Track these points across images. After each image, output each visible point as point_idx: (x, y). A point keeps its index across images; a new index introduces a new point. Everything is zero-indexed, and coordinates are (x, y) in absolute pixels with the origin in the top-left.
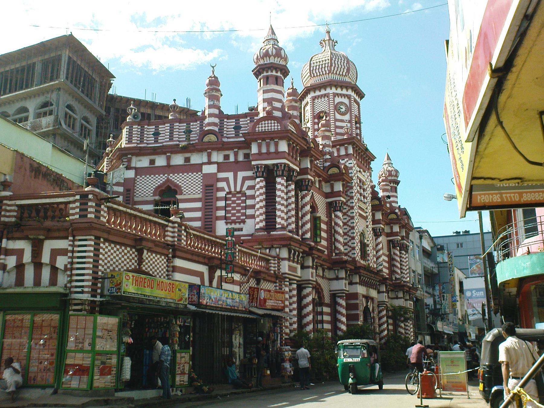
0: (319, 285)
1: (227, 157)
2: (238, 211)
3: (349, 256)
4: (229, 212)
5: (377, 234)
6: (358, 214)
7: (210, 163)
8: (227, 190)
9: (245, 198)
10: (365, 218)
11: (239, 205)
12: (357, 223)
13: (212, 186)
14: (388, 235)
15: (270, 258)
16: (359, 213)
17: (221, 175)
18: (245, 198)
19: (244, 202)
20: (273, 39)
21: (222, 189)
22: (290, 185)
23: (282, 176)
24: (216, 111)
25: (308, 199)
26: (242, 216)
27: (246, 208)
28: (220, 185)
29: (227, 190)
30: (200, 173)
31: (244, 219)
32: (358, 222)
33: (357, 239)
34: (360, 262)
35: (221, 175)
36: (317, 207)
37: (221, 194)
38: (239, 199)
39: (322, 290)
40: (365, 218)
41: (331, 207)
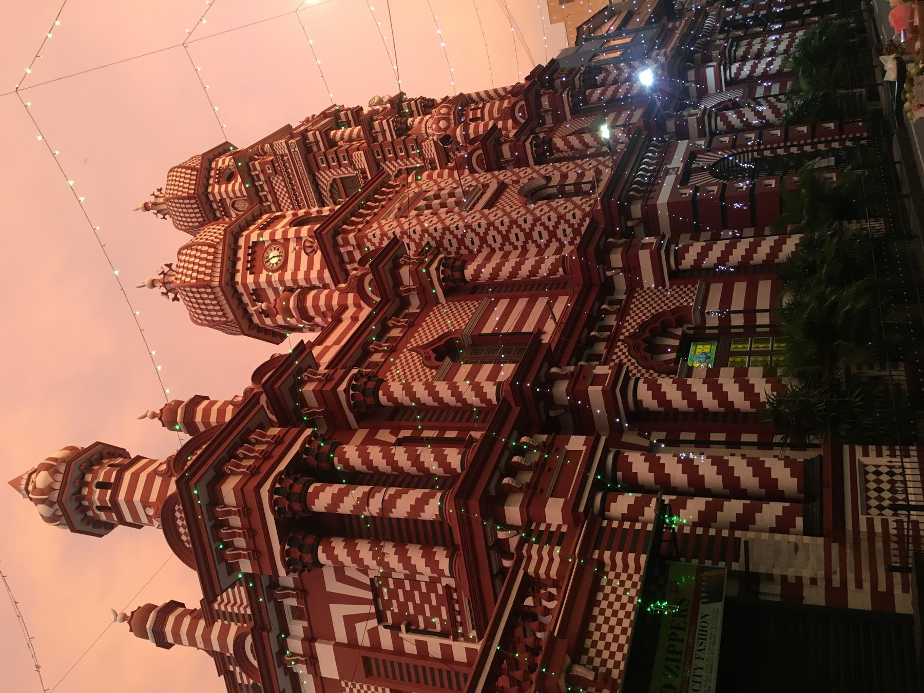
0: (643, 326)
6: (486, 211)
10: (502, 187)
15: (521, 573)
16: (484, 208)
20: (23, 485)
22: (345, 461)
23: (304, 499)
32: (503, 210)
33: (540, 209)
36: (440, 338)
39: (655, 318)
40: (502, 187)
41: (457, 288)
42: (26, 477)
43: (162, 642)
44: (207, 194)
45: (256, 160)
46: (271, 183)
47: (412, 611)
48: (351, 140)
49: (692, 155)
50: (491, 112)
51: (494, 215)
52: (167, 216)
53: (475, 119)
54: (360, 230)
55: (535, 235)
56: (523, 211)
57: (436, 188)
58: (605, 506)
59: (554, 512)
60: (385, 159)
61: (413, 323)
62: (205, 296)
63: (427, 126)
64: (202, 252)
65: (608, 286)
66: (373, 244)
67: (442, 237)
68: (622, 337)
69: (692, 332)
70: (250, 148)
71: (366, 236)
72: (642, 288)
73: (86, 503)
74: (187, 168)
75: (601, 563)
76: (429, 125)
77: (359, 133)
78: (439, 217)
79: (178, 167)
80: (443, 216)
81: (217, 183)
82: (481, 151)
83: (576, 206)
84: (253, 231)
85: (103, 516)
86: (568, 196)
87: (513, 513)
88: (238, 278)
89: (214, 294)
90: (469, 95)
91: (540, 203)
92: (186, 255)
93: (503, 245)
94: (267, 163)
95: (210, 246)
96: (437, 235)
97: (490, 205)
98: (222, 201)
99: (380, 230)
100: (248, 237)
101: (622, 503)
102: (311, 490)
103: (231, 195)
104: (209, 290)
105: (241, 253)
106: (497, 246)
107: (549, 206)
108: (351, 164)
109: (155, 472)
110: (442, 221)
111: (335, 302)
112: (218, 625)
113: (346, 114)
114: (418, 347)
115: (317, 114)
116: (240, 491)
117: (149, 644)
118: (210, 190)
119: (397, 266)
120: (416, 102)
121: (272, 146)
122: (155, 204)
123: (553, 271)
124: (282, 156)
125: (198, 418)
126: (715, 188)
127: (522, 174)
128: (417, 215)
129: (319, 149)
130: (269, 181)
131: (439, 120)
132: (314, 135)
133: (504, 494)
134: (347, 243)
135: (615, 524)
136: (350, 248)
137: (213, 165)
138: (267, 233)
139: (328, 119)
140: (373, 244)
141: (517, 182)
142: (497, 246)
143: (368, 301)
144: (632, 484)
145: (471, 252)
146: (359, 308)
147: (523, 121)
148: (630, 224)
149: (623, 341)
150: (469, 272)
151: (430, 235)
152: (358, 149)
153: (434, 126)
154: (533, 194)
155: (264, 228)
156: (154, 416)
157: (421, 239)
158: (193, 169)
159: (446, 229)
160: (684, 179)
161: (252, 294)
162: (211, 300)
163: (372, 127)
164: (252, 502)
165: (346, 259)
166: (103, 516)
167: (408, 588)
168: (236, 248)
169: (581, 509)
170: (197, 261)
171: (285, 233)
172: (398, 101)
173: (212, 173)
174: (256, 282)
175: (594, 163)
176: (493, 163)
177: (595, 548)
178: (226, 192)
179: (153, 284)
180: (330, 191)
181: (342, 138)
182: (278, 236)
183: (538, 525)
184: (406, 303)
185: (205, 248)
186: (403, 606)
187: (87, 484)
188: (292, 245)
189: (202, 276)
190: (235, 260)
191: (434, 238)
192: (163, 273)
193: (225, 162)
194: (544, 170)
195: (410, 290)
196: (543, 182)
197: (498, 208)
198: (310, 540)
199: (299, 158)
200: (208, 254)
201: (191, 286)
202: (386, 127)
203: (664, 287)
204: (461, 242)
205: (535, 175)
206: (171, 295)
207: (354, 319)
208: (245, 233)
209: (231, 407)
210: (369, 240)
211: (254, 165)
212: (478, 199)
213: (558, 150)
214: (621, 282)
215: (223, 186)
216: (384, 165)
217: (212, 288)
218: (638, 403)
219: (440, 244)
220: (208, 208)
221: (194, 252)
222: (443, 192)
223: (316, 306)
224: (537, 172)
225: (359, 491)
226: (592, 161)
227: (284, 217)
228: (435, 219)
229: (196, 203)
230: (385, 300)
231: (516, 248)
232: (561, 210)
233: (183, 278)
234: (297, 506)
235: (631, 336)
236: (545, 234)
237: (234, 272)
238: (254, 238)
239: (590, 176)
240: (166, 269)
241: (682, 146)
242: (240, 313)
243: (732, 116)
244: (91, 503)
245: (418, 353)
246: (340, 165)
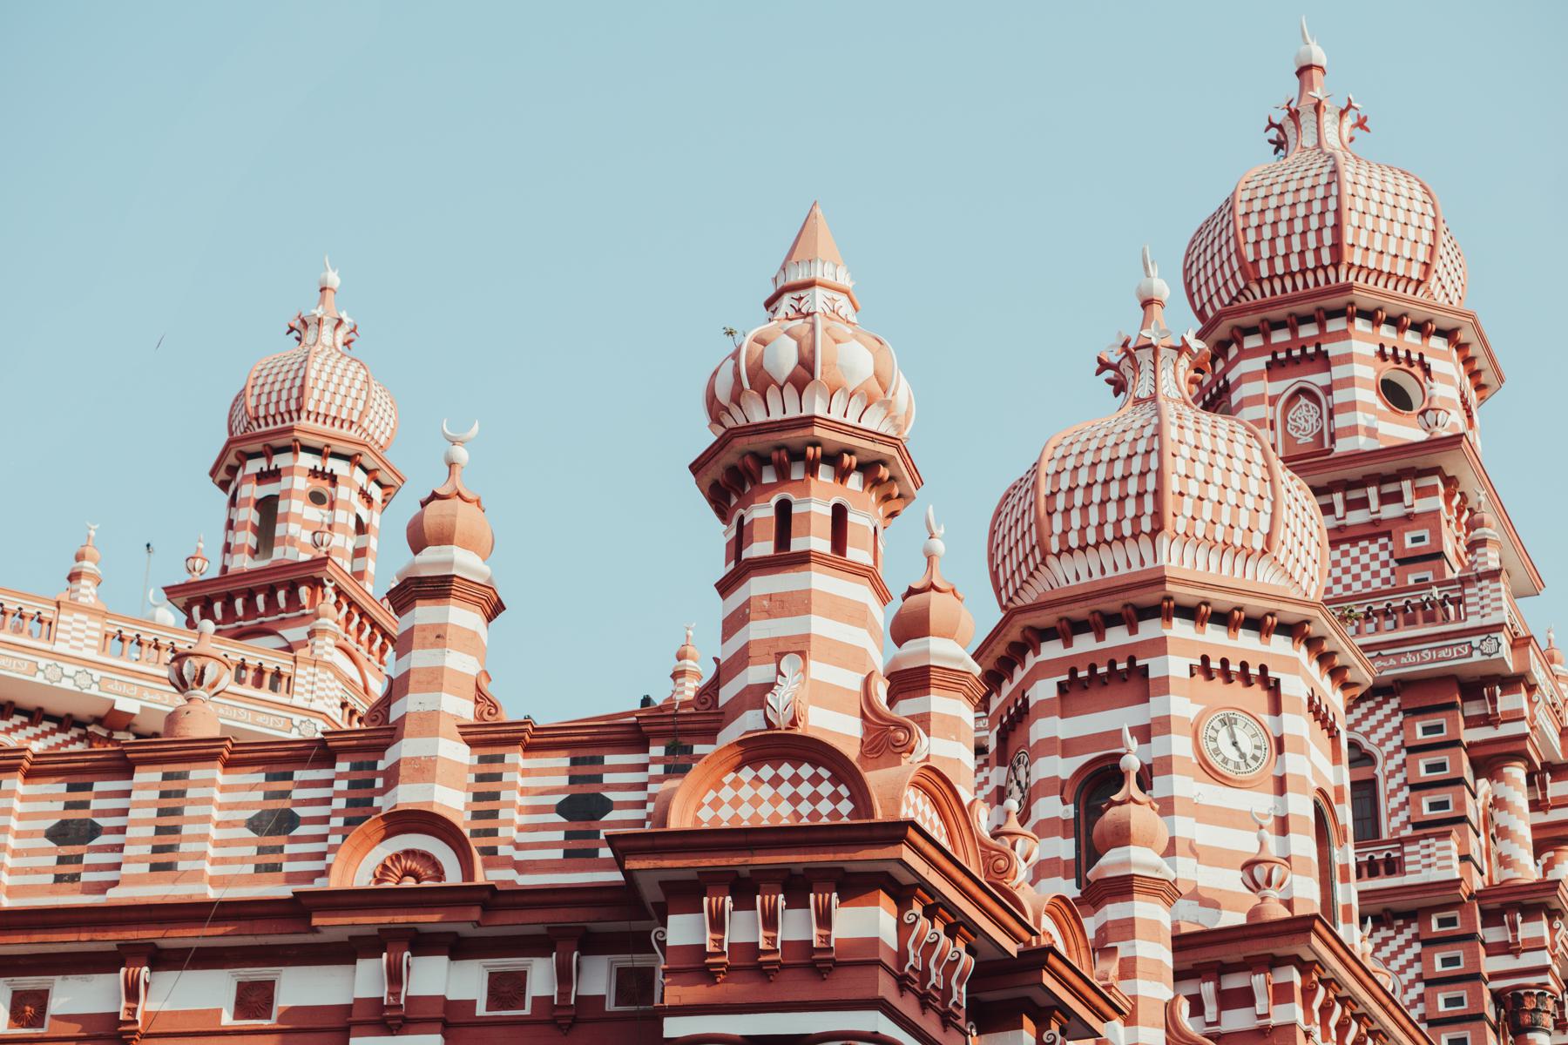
1: (506, 989)
44: (1348, 313)
45: (1448, 498)
46: (1373, 538)
52: (1274, 133)
60: (1430, 942)
84: (1308, 678)
89: (1135, 536)
94: (1437, 534)
98: (1322, 361)
100: (1293, 666)
134: (1282, 994)
136: (1262, 1004)
161: (1131, 660)
163: (1531, 913)
165: (1233, 982)
181: (1498, 803)
199: (1450, 659)
202: (1528, 960)
211: (1432, 491)
220: (1306, 308)
229: (1320, 266)
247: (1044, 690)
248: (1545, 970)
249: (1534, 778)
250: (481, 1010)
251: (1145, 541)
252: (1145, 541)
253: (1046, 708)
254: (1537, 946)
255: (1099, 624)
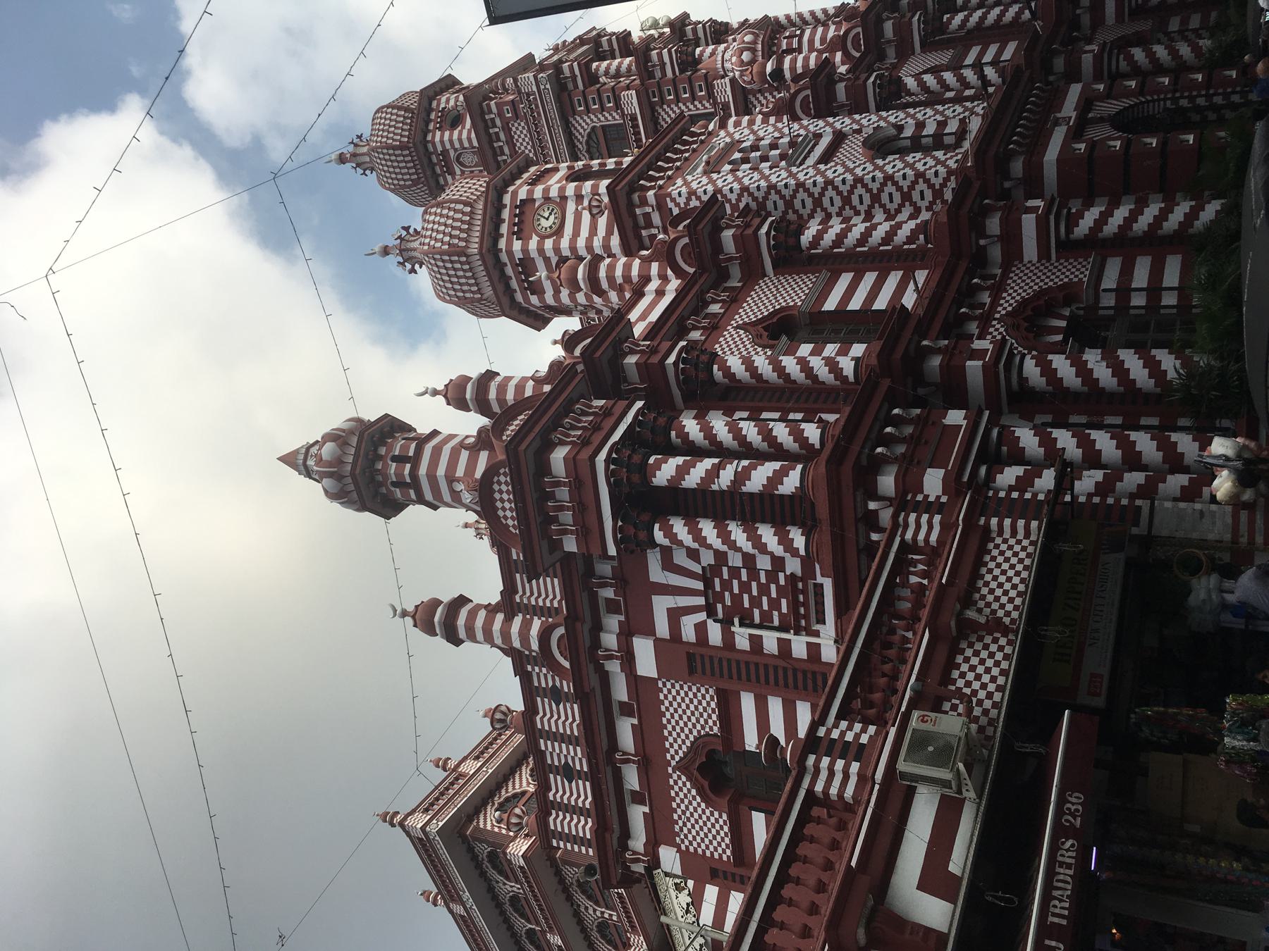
0: (1023, 304)
1: (613, 607)
2: (764, 590)
3: (943, 185)
4: (766, 617)
5: (892, 95)
6: (822, 167)
7: (628, 659)
8: (702, 616)
9: (725, 569)
11: (745, 587)
12: (847, 170)
13: (690, 657)
14: (905, 53)
15: (898, 539)
16: (820, 161)
17: (662, 629)
18: (725, 569)
19: (735, 572)
20: (298, 461)
21: (701, 629)
22: (684, 436)
23: (645, 472)
24: (500, 617)
25: (735, 364)
26: (777, 582)
27: (753, 572)
28: (689, 634)
29: (702, 616)
30: (660, 685)
31: (786, 576)
32: (843, 165)
33: (893, 165)
34: (965, 155)
35: (662, 629)
36: (776, 312)
37: (715, 634)
38: (727, 585)
39: (1039, 294)
40: (839, 138)
41: (791, 258)
42: (303, 451)
43: (455, 640)
44: (425, 142)
45: (492, 99)
47: (746, 605)
48: (618, 75)
49: (1086, 104)
50: (811, 41)
51: (833, 171)
52: (368, 172)
53: (789, 51)
54: (661, 187)
55: (885, 198)
56: (870, 167)
57: (752, 137)
58: (990, 477)
59: (933, 482)
60: (662, 101)
61: (735, 300)
62: (458, 266)
63: (726, 58)
64: (455, 211)
65: (980, 260)
66: (677, 205)
67: (766, 198)
68: (997, 316)
69: (1082, 312)
70: (486, 82)
71: (669, 195)
72: (1021, 261)
73: (380, 478)
74: (399, 108)
75: (987, 526)
76: (727, 56)
77: (630, 65)
78: (761, 173)
79: (388, 107)
80: (767, 172)
81: (439, 129)
82: (808, 92)
83: (938, 162)
84: (521, 186)
85: (398, 493)
86: (927, 151)
87: (887, 482)
88: (502, 244)
90: (776, 19)
91: (890, 158)
92: (436, 214)
93: (842, 209)
94: (506, 103)
95: (466, 204)
96: (760, 195)
97: (826, 158)
98: (445, 152)
99: (691, 184)
100: (515, 193)
101: (1010, 475)
102: (651, 461)
103: (457, 145)
104: (464, 259)
105: (506, 214)
106: (834, 210)
107: (904, 161)
108: (618, 106)
109: (462, 445)
110: (764, 177)
111: (635, 272)
112: (518, 621)
113: (610, 41)
114: (745, 324)
115: (570, 39)
116: (570, 461)
117: (439, 642)
118: (429, 138)
119: (717, 229)
120: (704, 26)
121: (515, 81)
122: (354, 155)
123: (911, 239)
124: (528, 95)
125: (492, 395)
126: (1118, 143)
127: (864, 122)
128: (731, 170)
129: (576, 87)
130: (507, 129)
131: (741, 51)
132: (571, 67)
133: (876, 466)
134: (644, 202)
135: (1002, 494)
136: (648, 209)
137: (434, 104)
138: (538, 191)
139: (585, 48)
140: (677, 205)
141: (859, 132)
142: (834, 210)
143: (679, 273)
144: (1018, 457)
145: (800, 217)
146: (664, 278)
147: (857, 55)
148: (1007, 185)
149: (999, 321)
150: (807, 237)
151: (751, 194)
152: (628, 88)
153: (734, 59)
154: (880, 146)
155: (534, 182)
156: (435, 393)
157: (739, 200)
158: (407, 110)
159: (772, 187)
160: (1076, 133)
161: (517, 265)
162: (464, 271)
163: (648, 58)
164: (584, 471)
165: (641, 221)
166: (398, 493)
167: (744, 578)
168: (500, 207)
169: (965, 479)
170: (450, 222)
171: (562, 189)
172: (680, 25)
173: (433, 116)
174: (525, 250)
175: (959, 109)
176: (824, 107)
177: (981, 515)
178: (451, 141)
179: (386, 251)
180: (587, 142)
181: (606, 73)
182: (554, 193)
183: (915, 496)
184: (724, 275)
185: (460, 207)
186: (737, 599)
187: (381, 458)
188: (571, 206)
189: (456, 241)
190: (498, 222)
191: (755, 199)
192: (400, 237)
193: (449, 101)
194: (893, 117)
195: (731, 259)
196: (893, 131)
197: (837, 164)
198: (646, 517)
199: (550, 98)
200: (463, 213)
201: (442, 253)
203: (1049, 259)
204: (789, 204)
205: (882, 124)
206: (409, 266)
207: (660, 293)
208: (511, 189)
209: (531, 383)
210: (673, 200)
211: (489, 105)
212: (810, 152)
213: (909, 93)
214: (996, 253)
215: (447, 134)
216: (753, 99)
217: (467, 256)
218: (1023, 380)
219: (762, 205)
220: (425, 161)
221: (445, 212)
222: (762, 143)
223: (611, 278)
224: (885, 119)
225: (708, 463)
226: (957, 107)
227: (556, 170)
228: (756, 176)
229: (410, 155)
230: (701, 270)
231: (857, 213)
232: (919, 166)
233: (432, 243)
234: (636, 478)
235: (1008, 314)
236: (897, 198)
237: (497, 236)
238: (522, 194)
239: (952, 127)
240: (404, 233)
241: (1075, 90)
242: (501, 288)
243: (1138, 54)
244: (386, 476)
245: (746, 331)
246: (602, 109)
247: (534, 299)
248: (669, 52)
249: (602, 58)
250: (622, 618)
251: (472, 259)
252: (472, 259)
253: (542, 299)
254: (660, 55)
255: (505, 279)
